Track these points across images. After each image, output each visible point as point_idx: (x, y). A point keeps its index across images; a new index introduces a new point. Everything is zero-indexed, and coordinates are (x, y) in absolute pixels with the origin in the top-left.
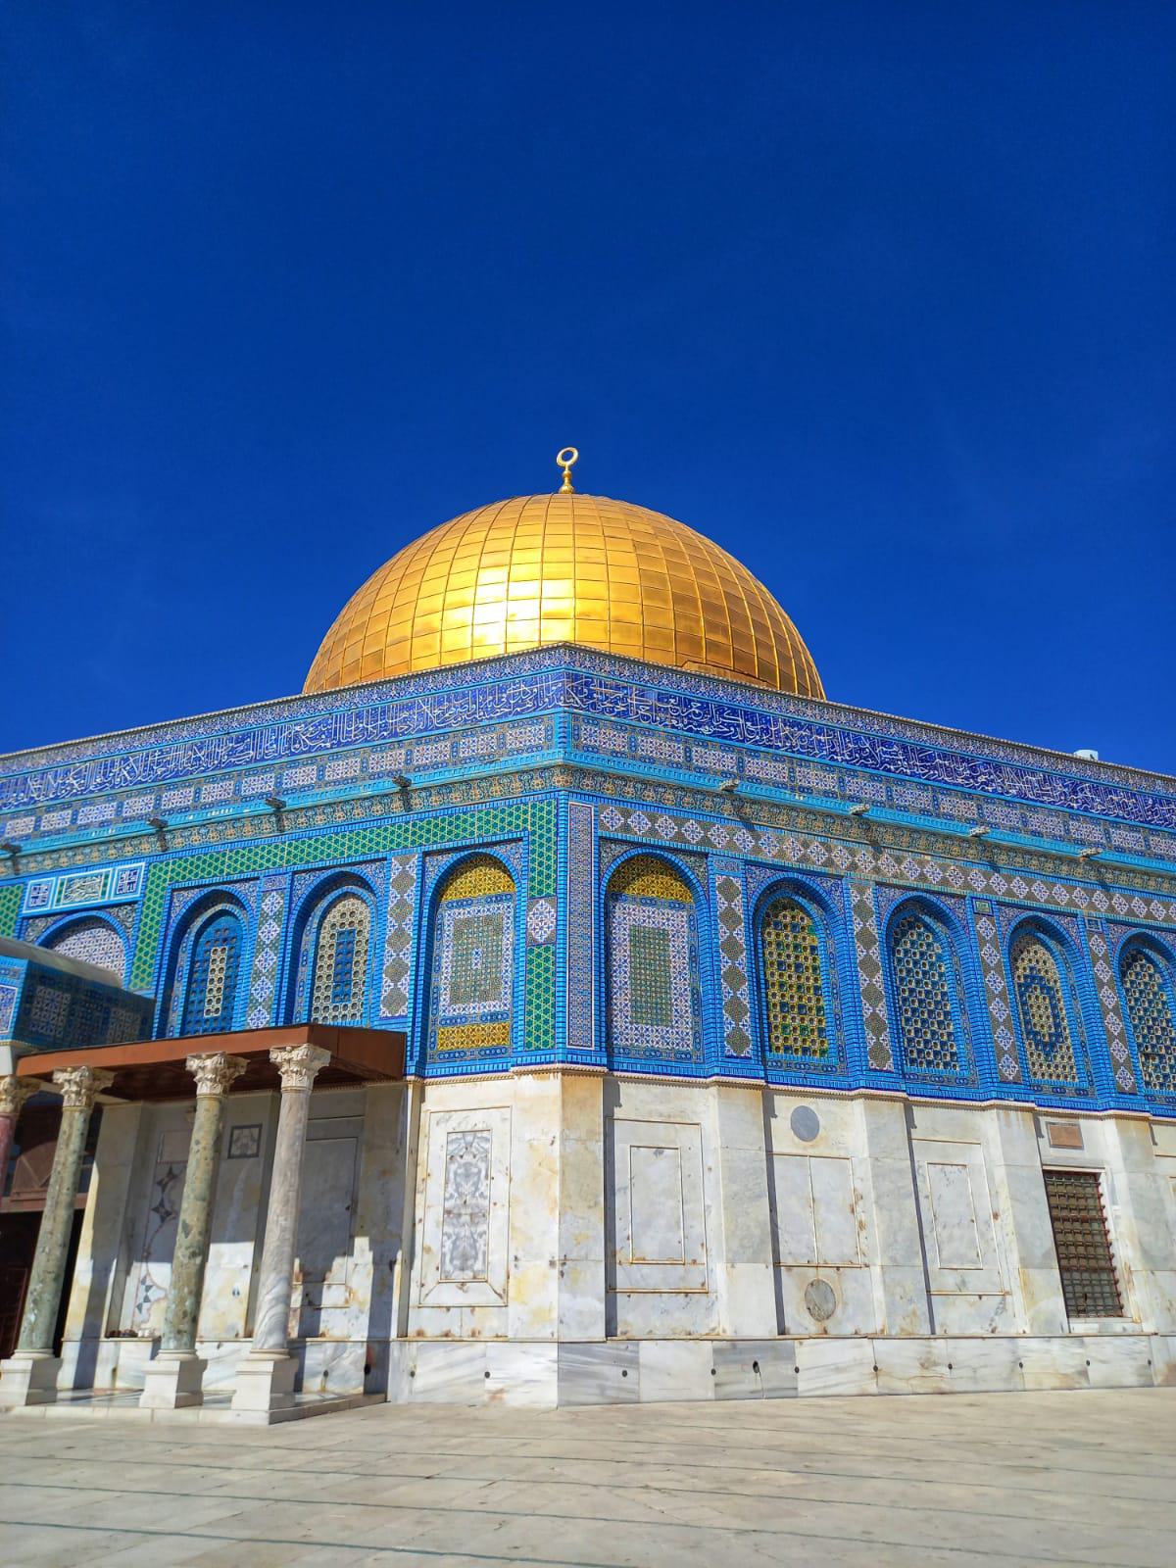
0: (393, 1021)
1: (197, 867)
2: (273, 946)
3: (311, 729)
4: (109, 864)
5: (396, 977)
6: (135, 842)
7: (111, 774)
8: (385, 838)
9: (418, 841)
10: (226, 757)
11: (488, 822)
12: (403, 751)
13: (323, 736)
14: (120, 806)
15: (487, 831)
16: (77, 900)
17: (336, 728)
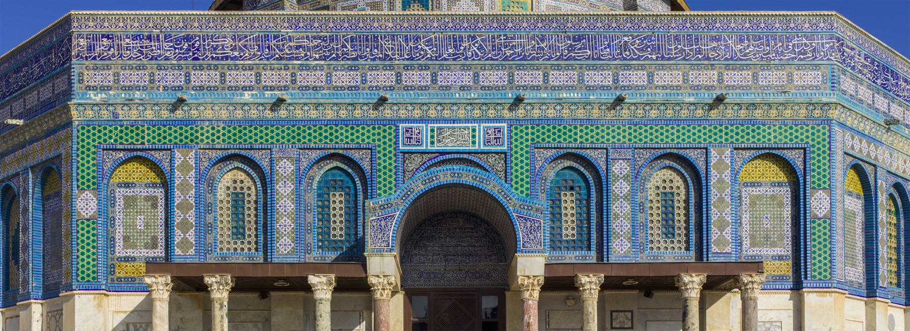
0: (721, 255)
1: (554, 134)
2: (625, 198)
3: (638, 42)
4: (474, 120)
5: (721, 228)
7: (462, 48)
8: (705, 134)
9: (730, 140)
10: (566, 51)
11: (781, 134)
12: (716, 73)
13: (649, 49)
14: (476, 75)
15: (781, 140)
16: (450, 145)
17: (659, 45)
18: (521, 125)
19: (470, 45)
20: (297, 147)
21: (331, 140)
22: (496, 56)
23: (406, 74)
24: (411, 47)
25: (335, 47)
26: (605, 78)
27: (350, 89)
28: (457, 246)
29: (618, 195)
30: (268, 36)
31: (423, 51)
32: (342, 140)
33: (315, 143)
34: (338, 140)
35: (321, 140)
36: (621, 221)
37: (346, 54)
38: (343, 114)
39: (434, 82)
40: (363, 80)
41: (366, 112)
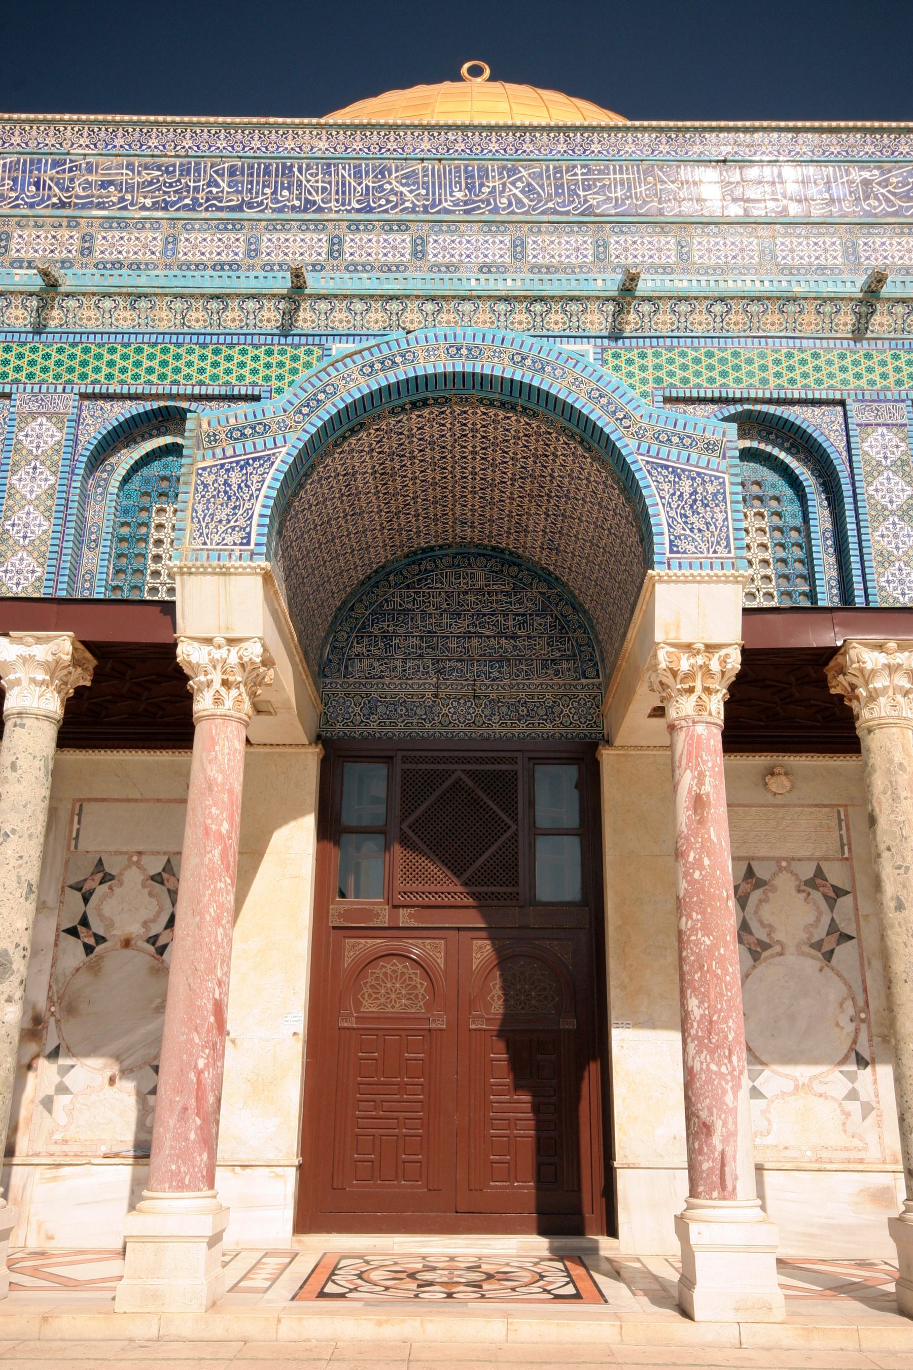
1: (711, 368)
6: (574, 307)
18: (630, 349)
19: (504, 185)
20: (76, 391)
21: (162, 377)
22: (564, 206)
23: (352, 240)
24: (367, 187)
25: (192, 184)
26: (826, 250)
27: (218, 267)
28: (468, 635)
29: (884, 508)
30: (40, 161)
31: (396, 194)
32: (188, 377)
33: (122, 383)
34: (179, 377)
35: (136, 377)
36: (900, 569)
37: (215, 199)
38: (197, 319)
39: (420, 255)
40: (250, 250)
41: (251, 317)
